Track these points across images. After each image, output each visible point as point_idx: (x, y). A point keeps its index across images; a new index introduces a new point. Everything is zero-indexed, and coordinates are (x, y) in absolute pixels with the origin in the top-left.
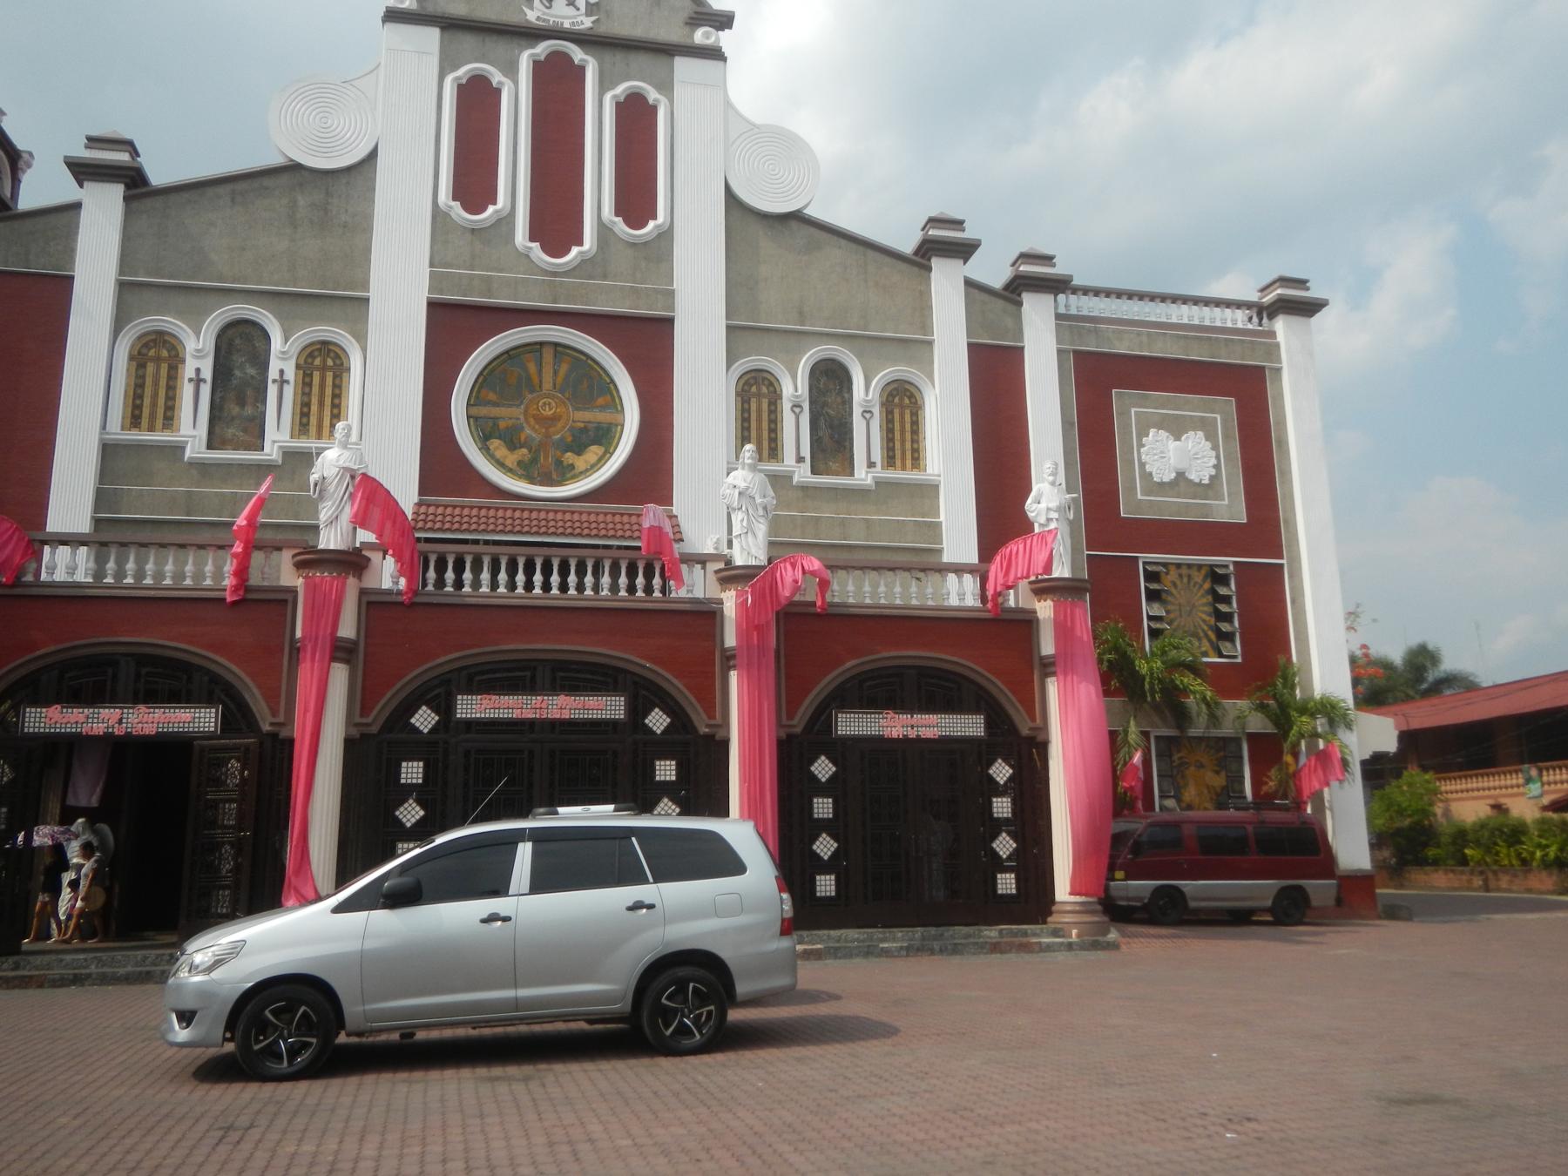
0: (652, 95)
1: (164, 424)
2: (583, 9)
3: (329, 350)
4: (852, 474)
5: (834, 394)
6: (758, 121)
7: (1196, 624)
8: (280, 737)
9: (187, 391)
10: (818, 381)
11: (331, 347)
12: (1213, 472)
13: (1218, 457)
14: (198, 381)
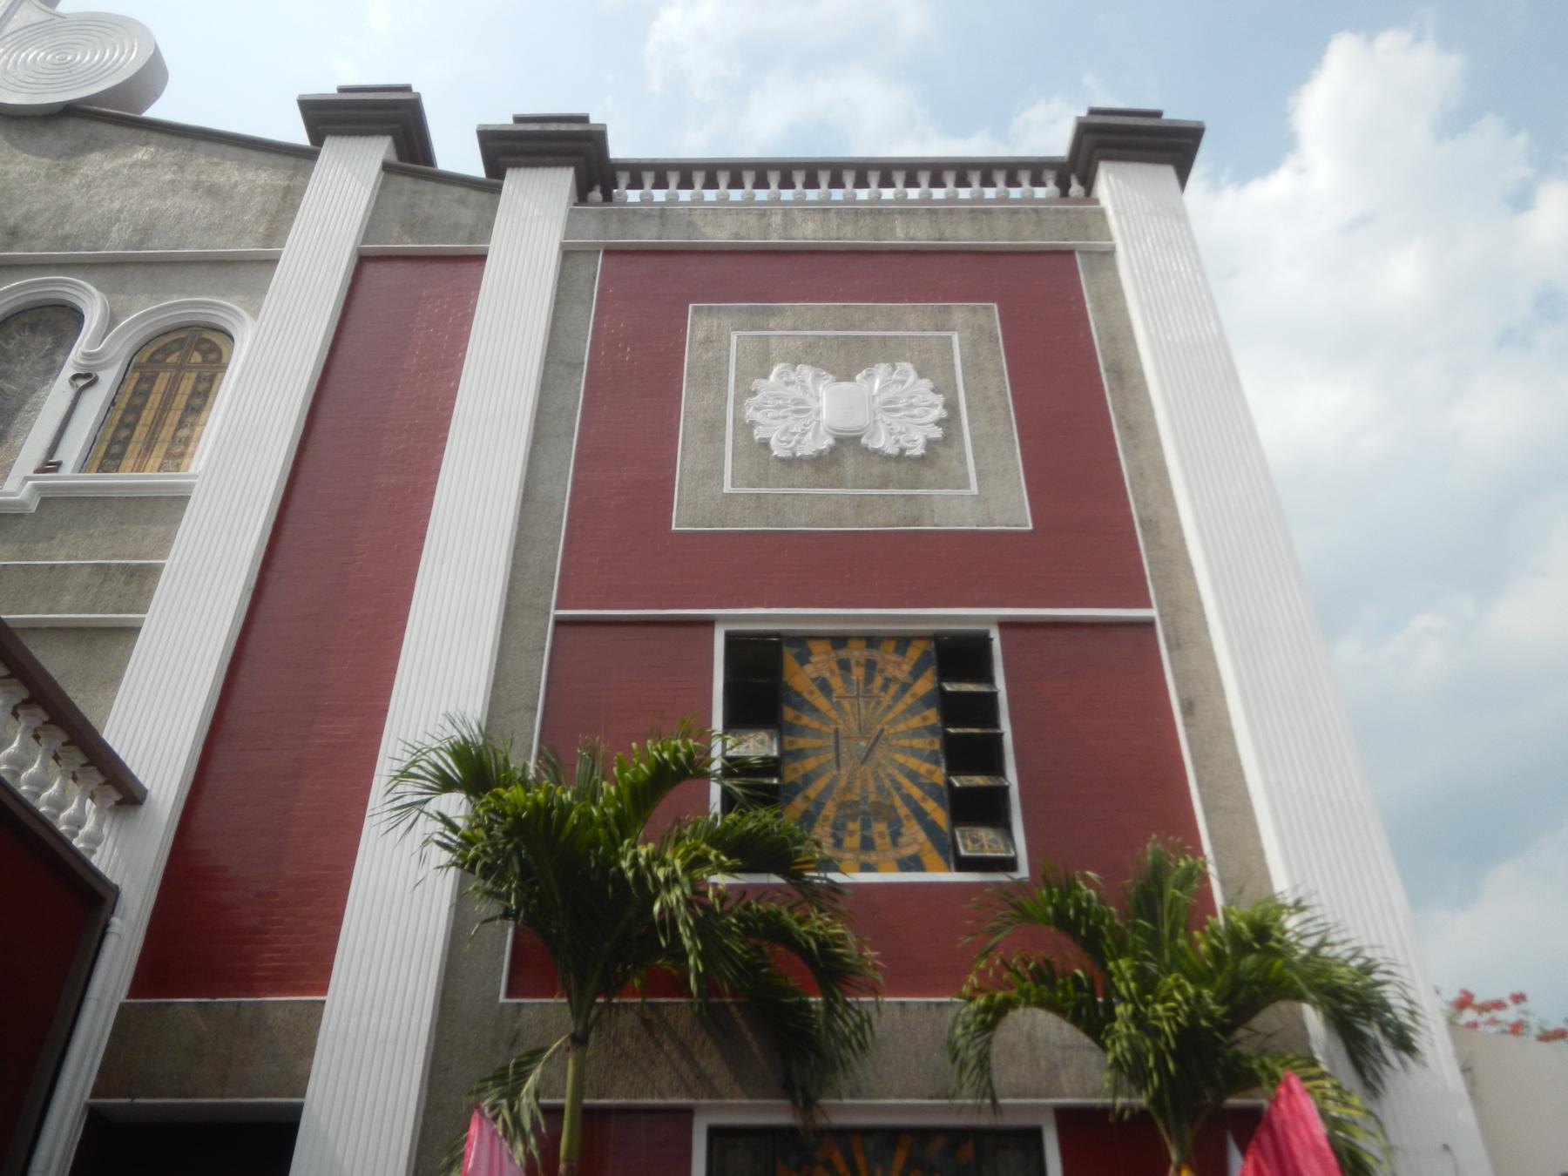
7: (887, 783)
13: (951, 406)
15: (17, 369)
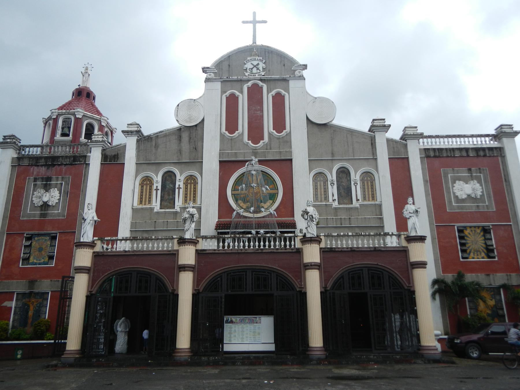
0: (283, 92)
1: (148, 203)
2: (261, 70)
3: (192, 178)
4: (352, 203)
5: (345, 178)
6: (316, 96)
8: (175, 294)
9: (154, 192)
10: (339, 174)
11: (193, 177)
12: (481, 194)
13: (482, 189)
14: (157, 190)
15: (343, 180)
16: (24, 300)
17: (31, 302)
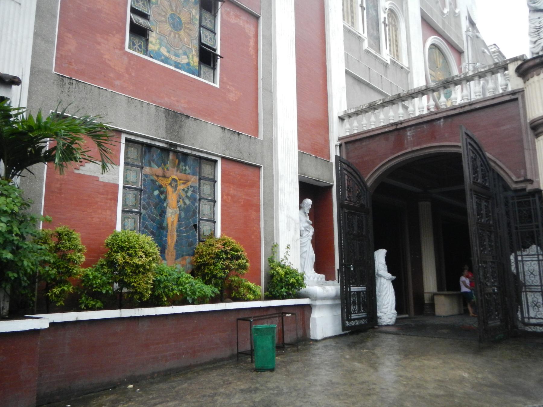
16: (147, 170)
17: (169, 182)
